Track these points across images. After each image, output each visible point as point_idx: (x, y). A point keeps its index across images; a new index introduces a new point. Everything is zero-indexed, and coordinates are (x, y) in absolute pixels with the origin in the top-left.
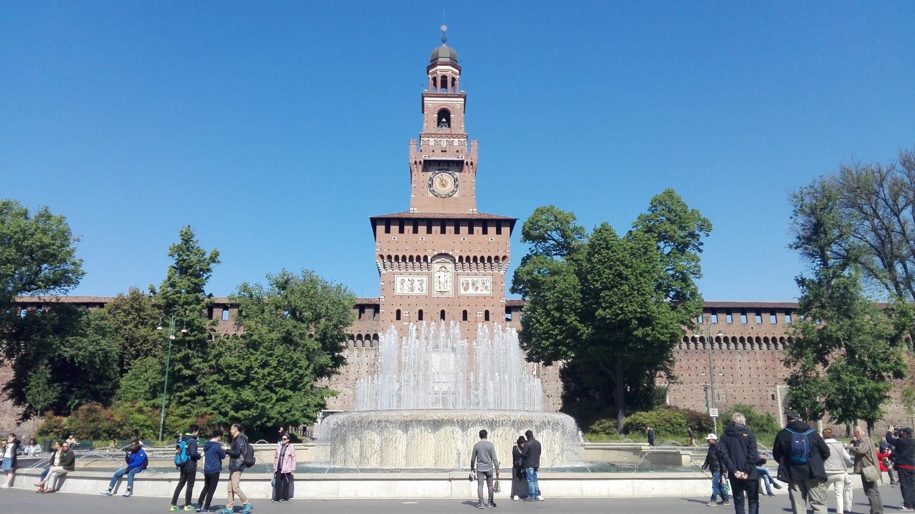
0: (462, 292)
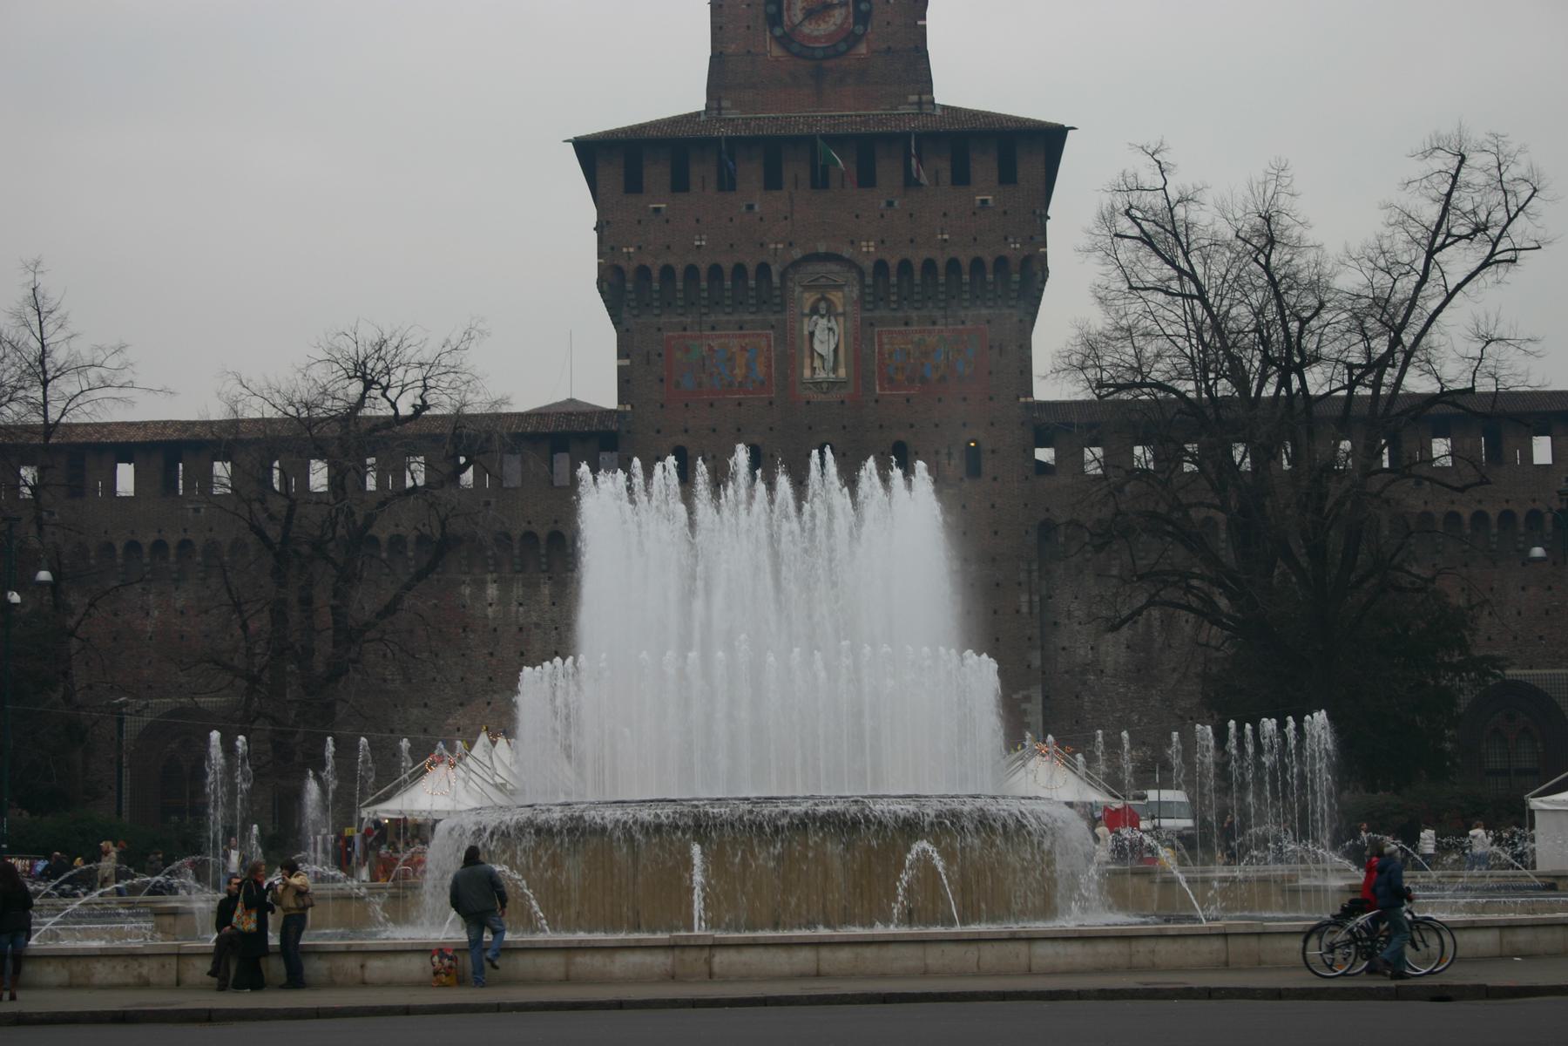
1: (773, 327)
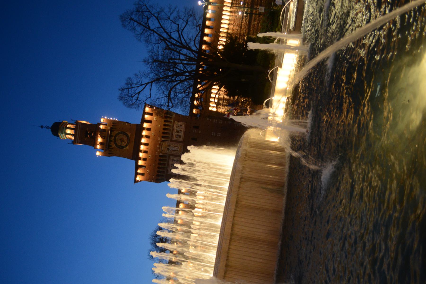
0: (181, 139)
1: (170, 156)
